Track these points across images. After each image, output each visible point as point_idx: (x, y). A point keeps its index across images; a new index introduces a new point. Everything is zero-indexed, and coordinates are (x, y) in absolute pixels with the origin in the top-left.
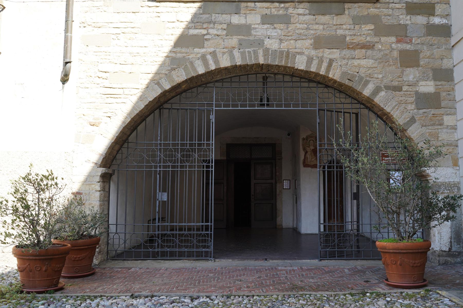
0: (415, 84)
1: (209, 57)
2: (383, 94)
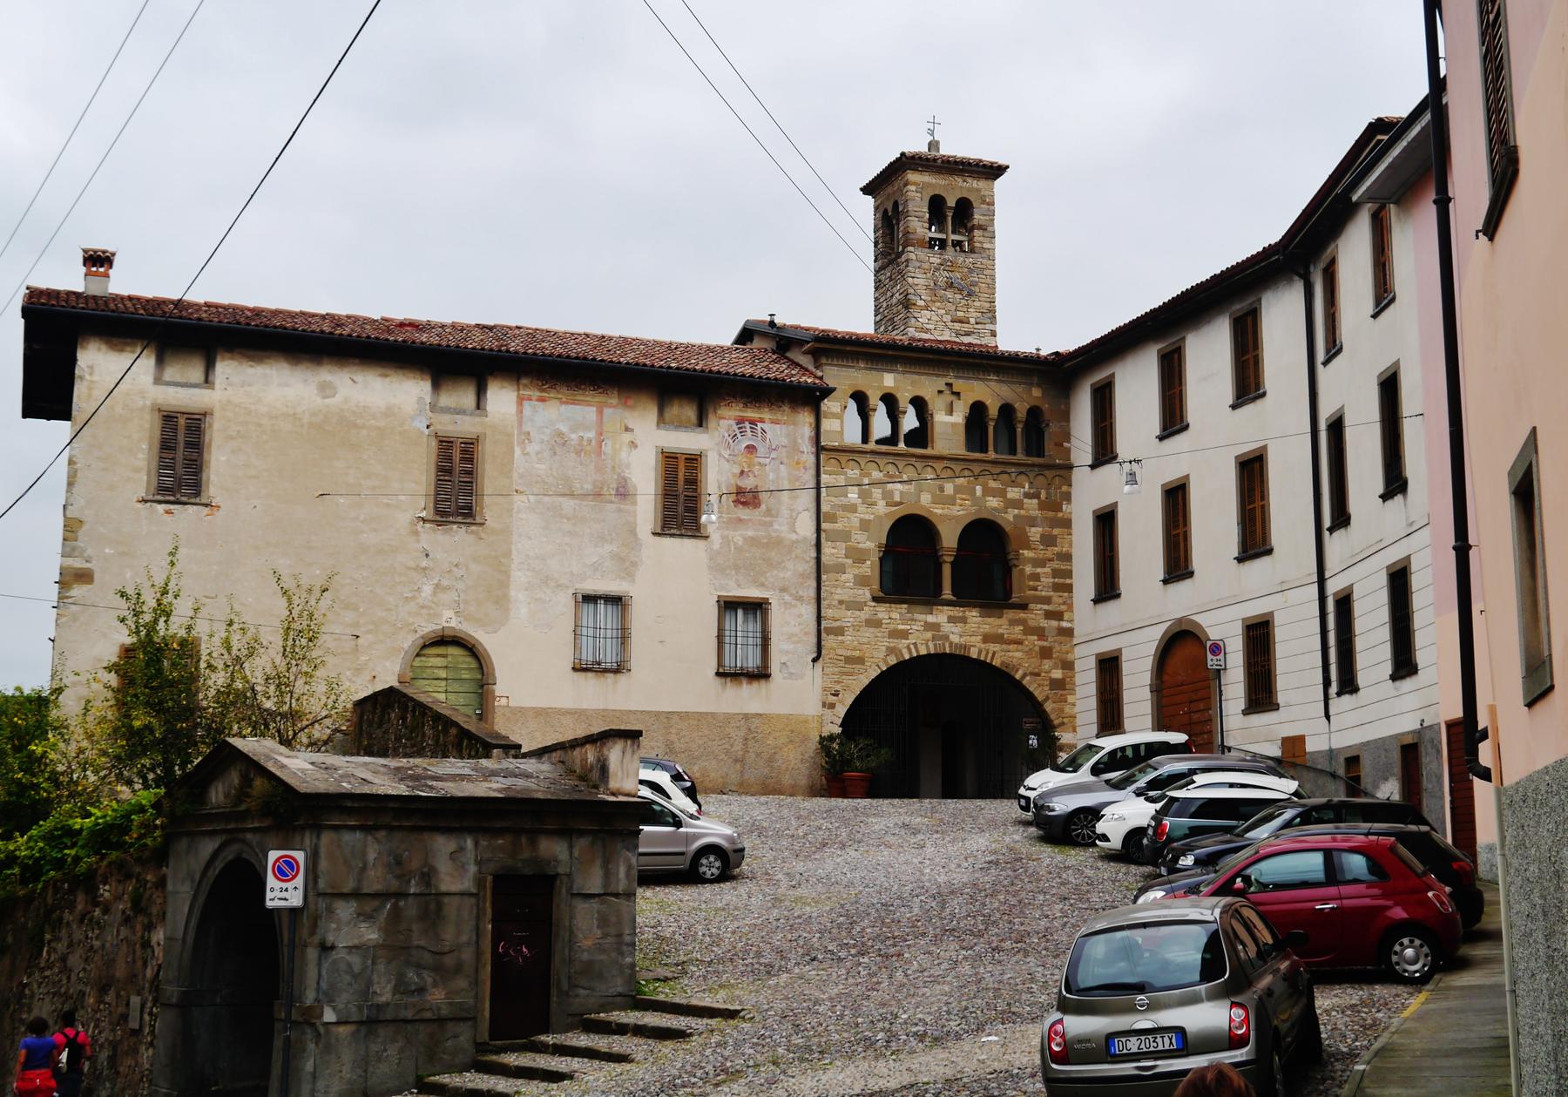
0: (1049, 672)
1: (912, 646)
2: (1028, 678)
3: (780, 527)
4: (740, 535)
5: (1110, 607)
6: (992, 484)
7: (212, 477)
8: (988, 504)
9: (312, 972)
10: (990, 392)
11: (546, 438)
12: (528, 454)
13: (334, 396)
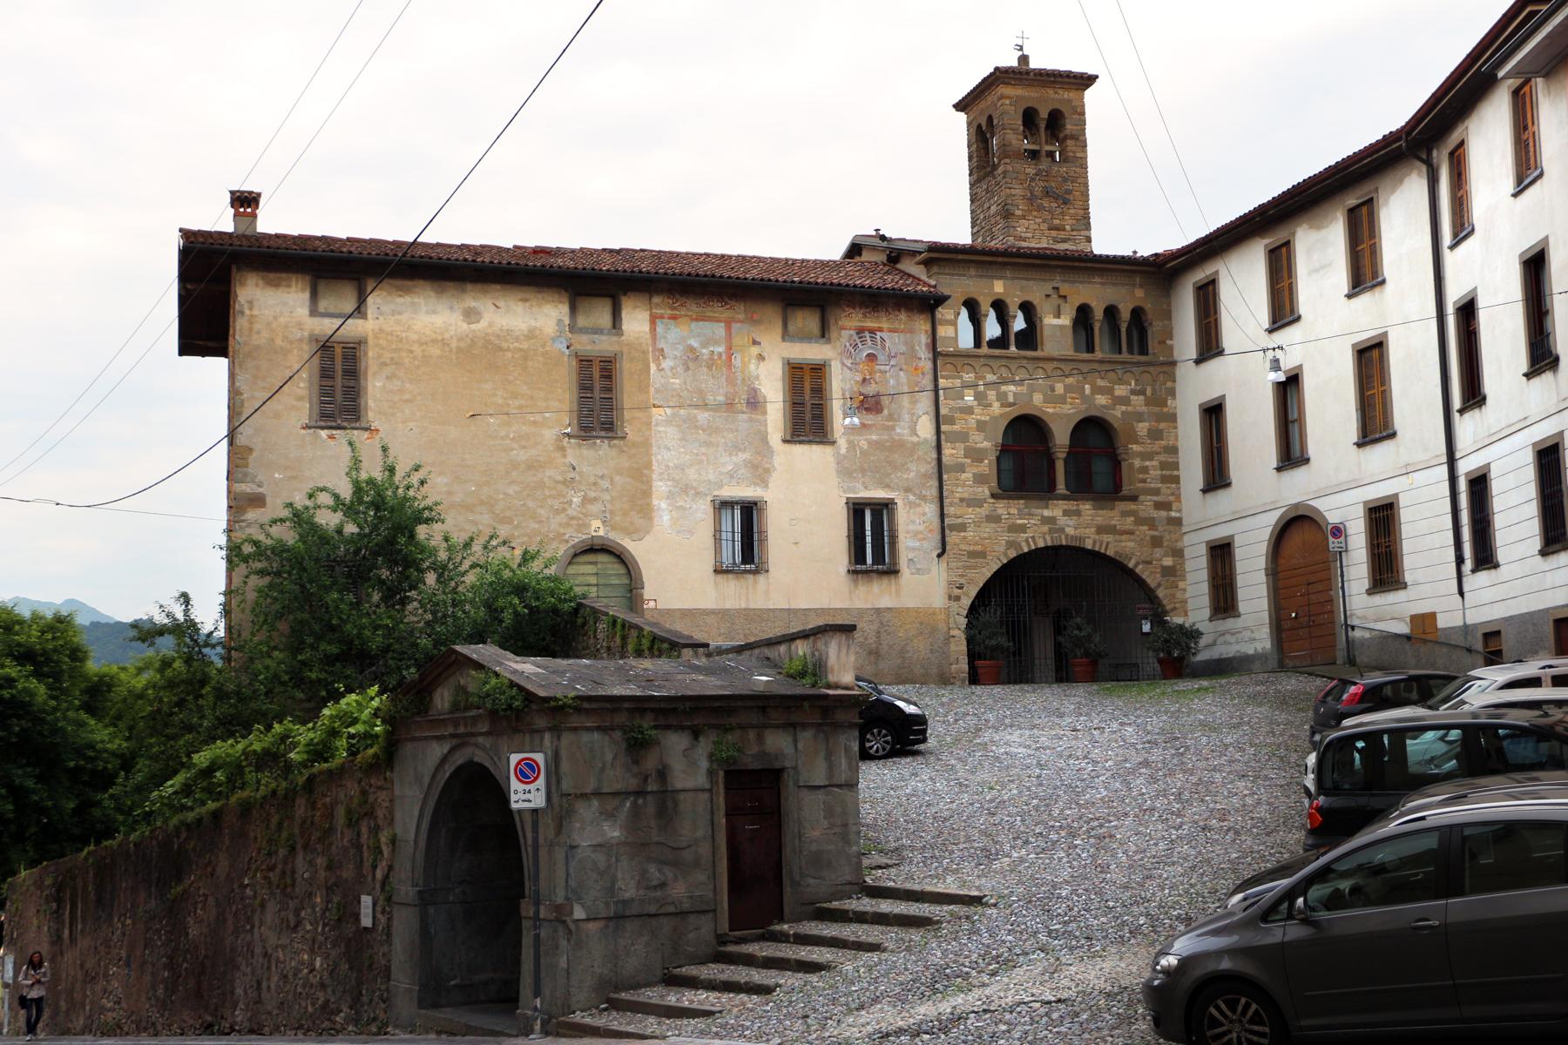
0: (1161, 560)
2: (1140, 567)
3: (902, 430)
4: (866, 440)
5: (1222, 495)
6: (1100, 383)
7: (371, 403)
8: (1097, 402)
9: (560, 873)
10: (1096, 295)
11: (679, 355)
12: (663, 369)
13: (478, 322)
